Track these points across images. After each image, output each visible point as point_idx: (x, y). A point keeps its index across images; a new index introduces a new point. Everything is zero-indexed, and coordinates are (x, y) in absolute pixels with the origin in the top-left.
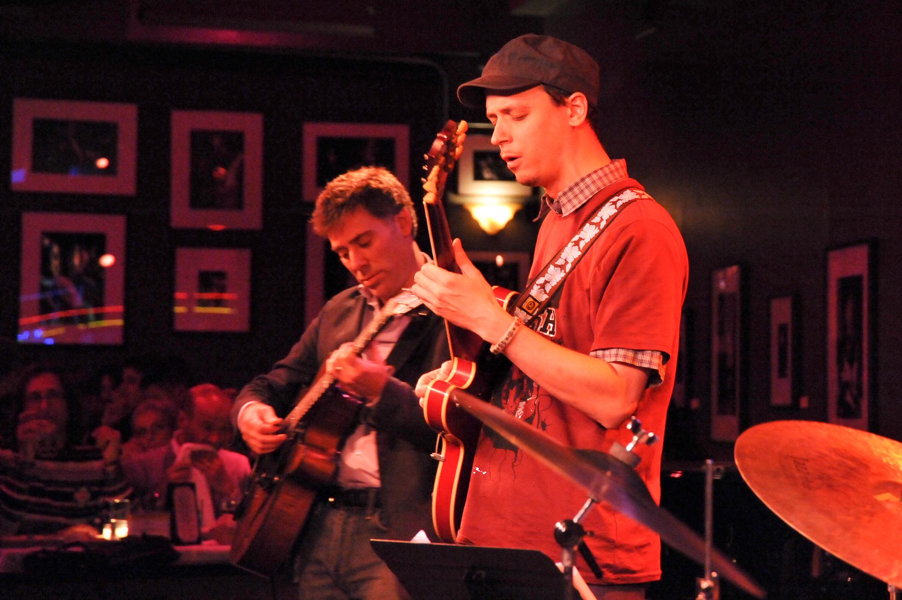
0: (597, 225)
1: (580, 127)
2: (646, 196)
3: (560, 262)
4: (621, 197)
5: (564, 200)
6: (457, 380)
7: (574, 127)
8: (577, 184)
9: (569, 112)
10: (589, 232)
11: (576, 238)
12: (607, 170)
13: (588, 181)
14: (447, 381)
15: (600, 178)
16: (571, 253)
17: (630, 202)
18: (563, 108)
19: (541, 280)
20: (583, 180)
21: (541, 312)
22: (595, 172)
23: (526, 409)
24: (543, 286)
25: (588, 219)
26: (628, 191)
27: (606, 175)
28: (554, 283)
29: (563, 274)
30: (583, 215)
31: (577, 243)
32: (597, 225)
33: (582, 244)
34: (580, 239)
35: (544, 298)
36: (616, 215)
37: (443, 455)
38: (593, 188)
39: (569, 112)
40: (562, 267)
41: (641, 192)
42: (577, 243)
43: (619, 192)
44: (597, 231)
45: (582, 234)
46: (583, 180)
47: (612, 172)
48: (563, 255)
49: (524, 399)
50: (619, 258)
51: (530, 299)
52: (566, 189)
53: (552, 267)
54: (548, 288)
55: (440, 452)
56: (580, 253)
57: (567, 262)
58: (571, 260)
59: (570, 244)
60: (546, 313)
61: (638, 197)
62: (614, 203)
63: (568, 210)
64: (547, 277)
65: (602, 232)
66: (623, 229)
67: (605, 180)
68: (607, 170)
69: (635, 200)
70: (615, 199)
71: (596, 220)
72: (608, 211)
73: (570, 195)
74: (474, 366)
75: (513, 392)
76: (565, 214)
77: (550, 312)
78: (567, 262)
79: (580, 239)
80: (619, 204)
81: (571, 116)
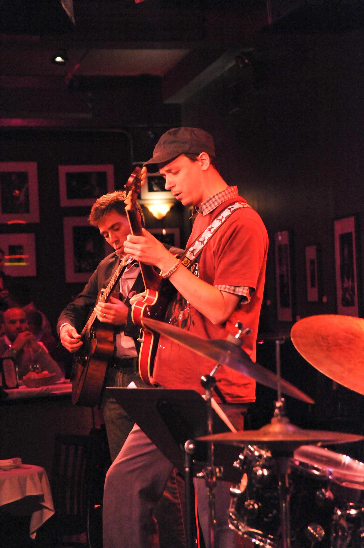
0: (221, 220)
1: (207, 170)
2: (247, 205)
3: (201, 239)
4: (233, 206)
5: (204, 207)
6: (148, 300)
7: (204, 171)
8: (211, 199)
9: (200, 163)
10: (216, 224)
11: (209, 227)
12: (227, 192)
13: (217, 197)
14: (143, 301)
15: (223, 196)
16: (207, 235)
17: (238, 209)
18: (196, 162)
19: (191, 249)
20: (214, 197)
21: (192, 265)
22: (221, 193)
23: (184, 315)
24: (192, 252)
25: (216, 217)
26: (237, 203)
27: (226, 194)
28: (198, 250)
29: (202, 246)
30: (214, 214)
31: (210, 230)
32: (221, 220)
33: (212, 230)
34: (212, 227)
35: (193, 258)
36: (230, 215)
37: (143, 339)
38: (219, 201)
39: (200, 163)
40: (202, 242)
41: (244, 203)
42: (210, 230)
43: (233, 204)
44: (220, 223)
45: (213, 225)
46: (214, 197)
47: (229, 193)
48: (203, 236)
49: (182, 309)
50: (229, 238)
51: (186, 259)
52: (205, 201)
53: (197, 242)
54: (195, 253)
55: (141, 338)
56: (211, 235)
57: (205, 240)
58: (207, 238)
59: (206, 230)
60: (194, 266)
61: (242, 206)
62: (230, 209)
63: (206, 212)
64: (194, 247)
65: (223, 224)
66: (233, 223)
67: (226, 197)
68: (227, 192)
69: (240, 208)
70: (230, 207)
71: (220, 217)
72: (226, 213)
73: (207, 204)
74: (157, 293)
75: (177, 306)
76: (204, 214)
77: (196, 265)
78: (205, 240)
79: (212, 227)
80: (232, 210)
81: (202, 165)
